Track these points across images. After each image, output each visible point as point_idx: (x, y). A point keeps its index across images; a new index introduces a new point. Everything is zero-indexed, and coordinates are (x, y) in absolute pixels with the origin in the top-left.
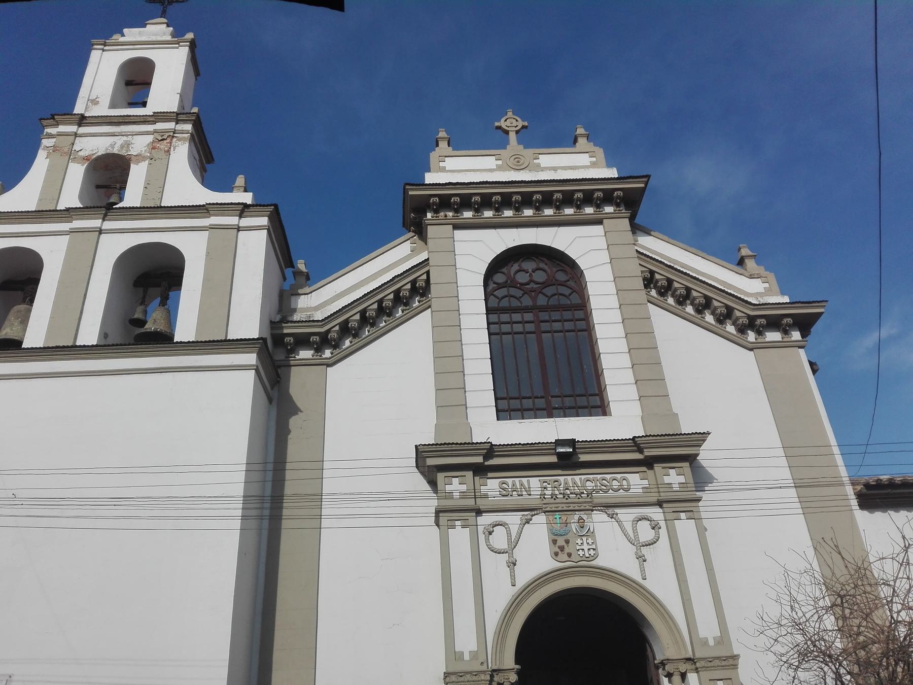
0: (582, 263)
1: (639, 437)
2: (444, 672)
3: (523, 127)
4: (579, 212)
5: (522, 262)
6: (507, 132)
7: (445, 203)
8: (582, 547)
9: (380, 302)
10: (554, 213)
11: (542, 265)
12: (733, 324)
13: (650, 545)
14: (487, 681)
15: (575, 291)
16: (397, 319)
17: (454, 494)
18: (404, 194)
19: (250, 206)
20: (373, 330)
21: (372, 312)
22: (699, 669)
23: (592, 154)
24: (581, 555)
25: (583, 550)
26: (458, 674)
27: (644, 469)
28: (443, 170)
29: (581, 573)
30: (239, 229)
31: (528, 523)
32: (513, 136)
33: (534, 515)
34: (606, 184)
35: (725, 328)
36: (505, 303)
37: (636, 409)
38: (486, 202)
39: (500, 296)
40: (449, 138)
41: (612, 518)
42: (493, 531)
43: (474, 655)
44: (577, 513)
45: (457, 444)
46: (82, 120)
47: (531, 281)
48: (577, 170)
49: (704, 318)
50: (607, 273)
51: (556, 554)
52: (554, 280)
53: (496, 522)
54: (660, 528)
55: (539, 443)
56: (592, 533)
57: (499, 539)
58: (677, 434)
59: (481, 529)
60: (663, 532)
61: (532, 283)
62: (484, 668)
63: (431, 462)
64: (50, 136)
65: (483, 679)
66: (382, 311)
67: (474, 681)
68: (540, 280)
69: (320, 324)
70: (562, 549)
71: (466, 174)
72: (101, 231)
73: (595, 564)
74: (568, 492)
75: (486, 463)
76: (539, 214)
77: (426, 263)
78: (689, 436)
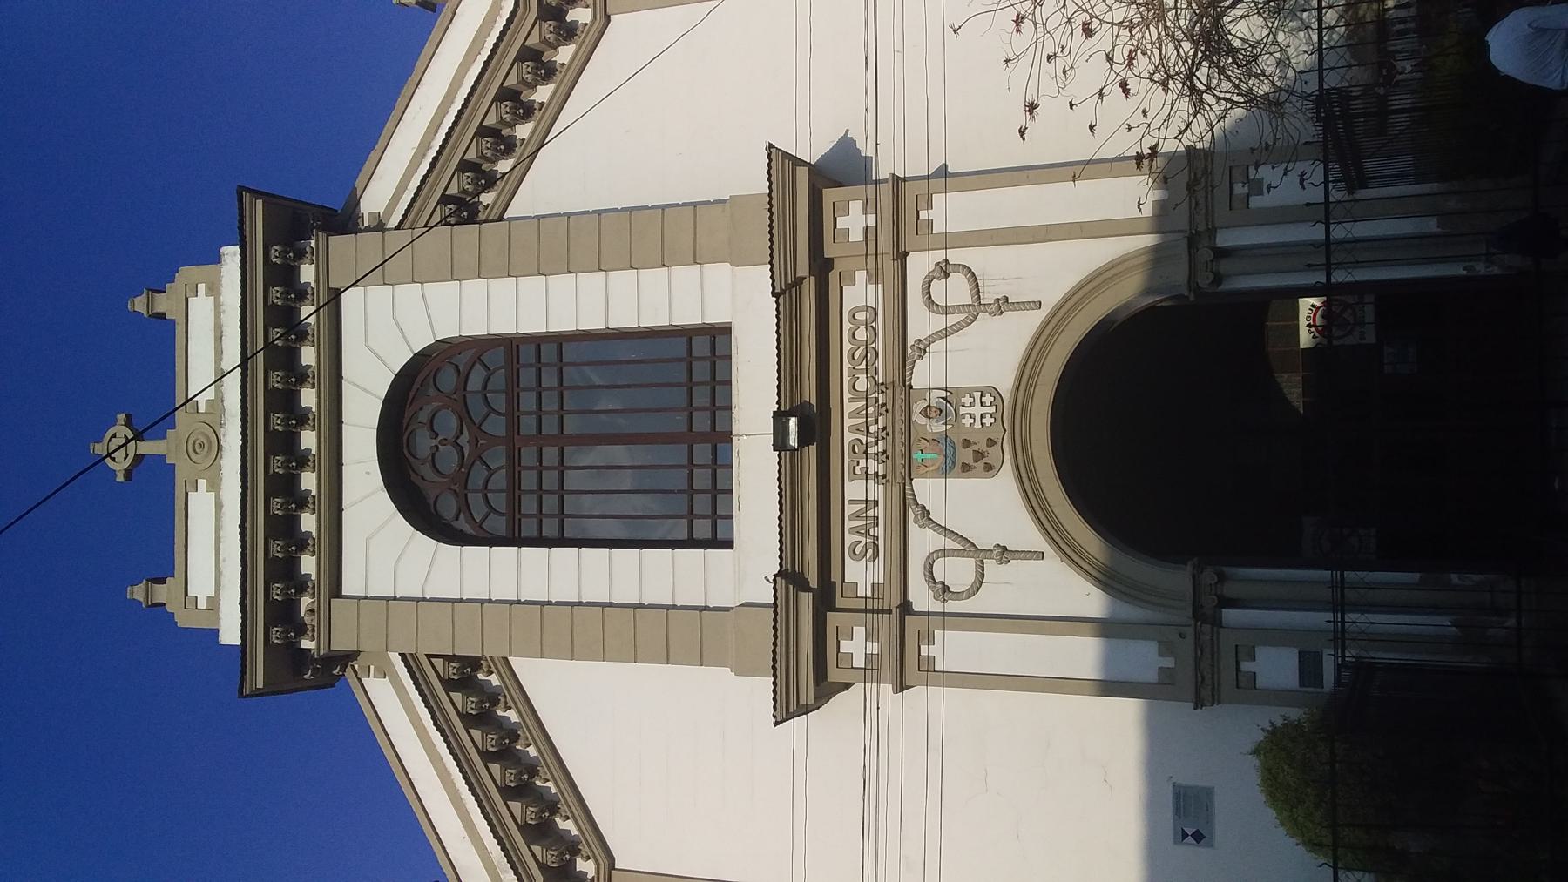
0: (421, 342)
1: (773, 285)
2: (1195, 709)
3: (128, 423)
4: (313, 336)
5: (415, 457)
6: (139, 459)
7: (283, 614)
8: (976, 413)
9: (487, 757)
10: (314, 388)
11: (423, 417)
12: (555, 48)
13: (977, 286)
14: (1213, 630)
15: (479, 358)
16: (523, 719)
17: (869, 652)
18: (261, 695)
20: (542, 769)
21: (508, 775)
22: (1210, 227)
23: (190, 291)
24: (992, 421)
25: (982, 416)
26: (1199, 684)
27: (833, 277)
28: (214, 602)
29: (1025, 424)
31: (929, 513)
32: (147, 447)
33: (915, 500)
34: (254, 281)
35: (563, 64)
36: (499, 501)
37: (720, 273)
38: (284, 528)
39: (486, 510)
40: (147, 580)
41: (925, 352)
42: (943, 583)
43: (1166, 649)
44: (913, 418)
45: (775, 644)
48: (224, 329)
49: (542, 104)
50: (443, 293)
51: (989, 467)
52: (455, 396)
53: (925, 575)
54: (946, 261)
55: (779, 479)
56: (951, 393)
57: (957, 572)
58: (770, 203)
59: (937, 607)
60: (955, 256)
61: (458, 441)
62: (1190, 631)
63: (808, 695)
65: (1208, 638)
66: (505, 754)
67: (1213, 655)
68: (454, 423)
70: (979, 455)
71: (224, 560)
73: (1009, 395)
74: (872, 429)
75: (814, 583)
76: (314, 419)
77: (409, 658)
78: (775, 218)
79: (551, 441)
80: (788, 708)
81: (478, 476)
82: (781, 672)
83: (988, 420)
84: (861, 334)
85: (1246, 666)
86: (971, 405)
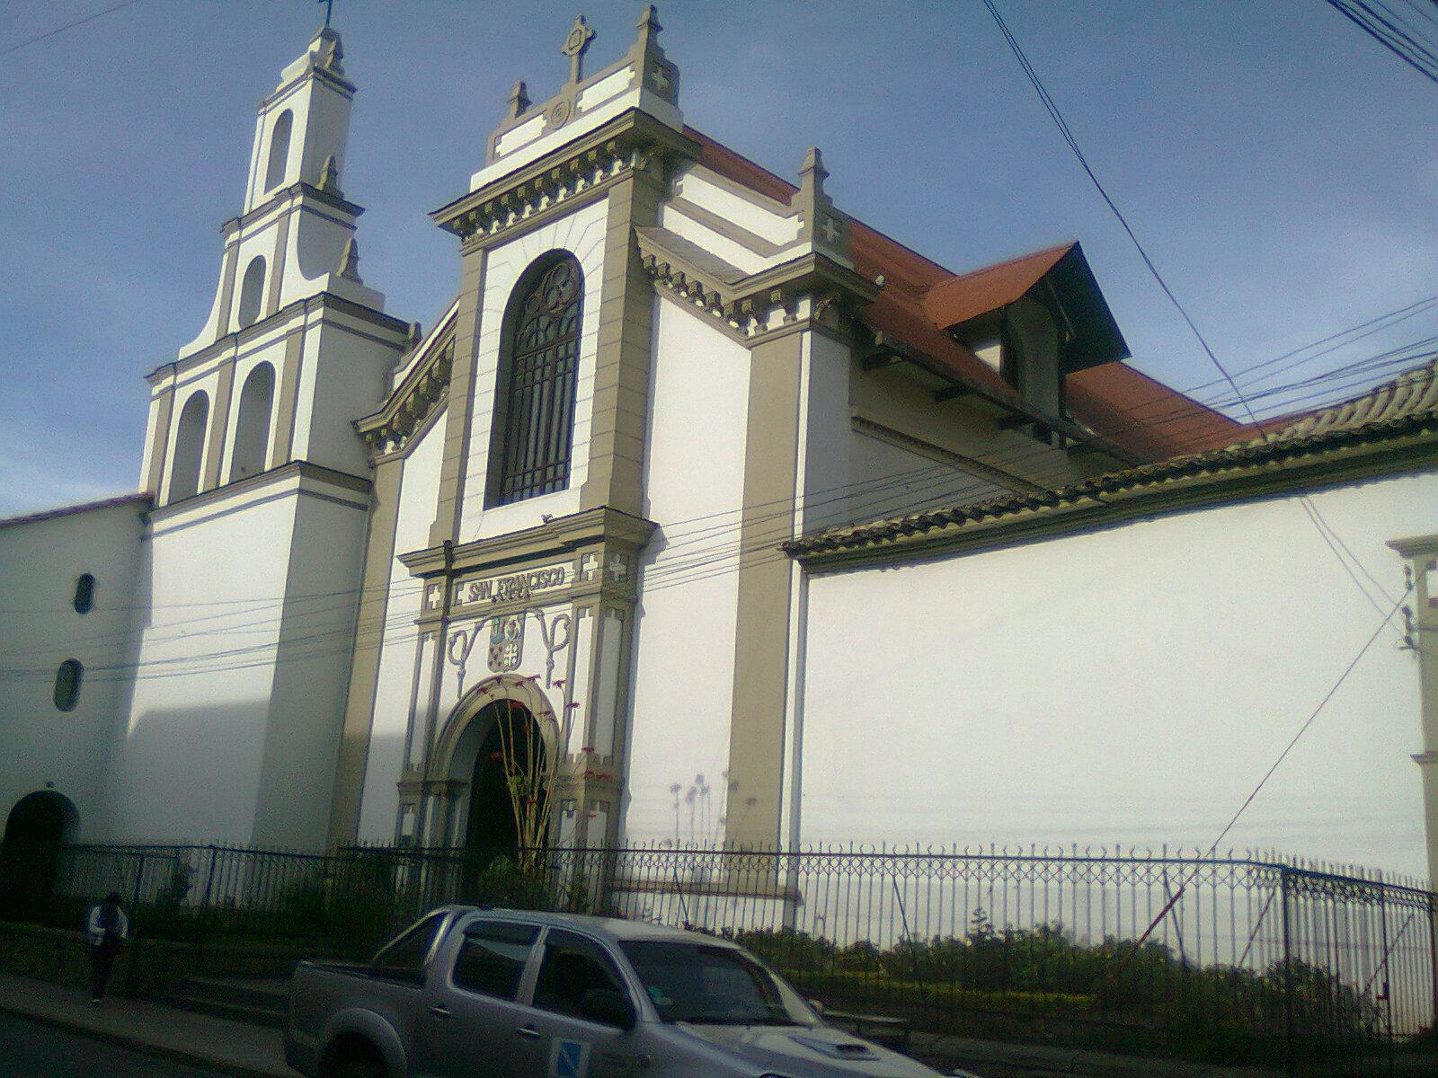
0: (585, 269)
3: (589, 40)
8: (509, 654)
9: (429, 372)
19: (308, 300)
25: (508, 658)
28: (496, 158)
30: (304, 329)
33: (484, 621)
42: (455, 641)
46: (240, 223)
47: (557, 305)
51: (490, 664)
64: (226, 251)
69: (380, 416)
70: (495, 658)
72: (234, 360)
79: (555, 369)
80: (409, 560)
81: (544, 321)
82: (429, 553)
83: (506, 662)
84: (553, 577)
85: (411, 808)
86: (513, 652)
